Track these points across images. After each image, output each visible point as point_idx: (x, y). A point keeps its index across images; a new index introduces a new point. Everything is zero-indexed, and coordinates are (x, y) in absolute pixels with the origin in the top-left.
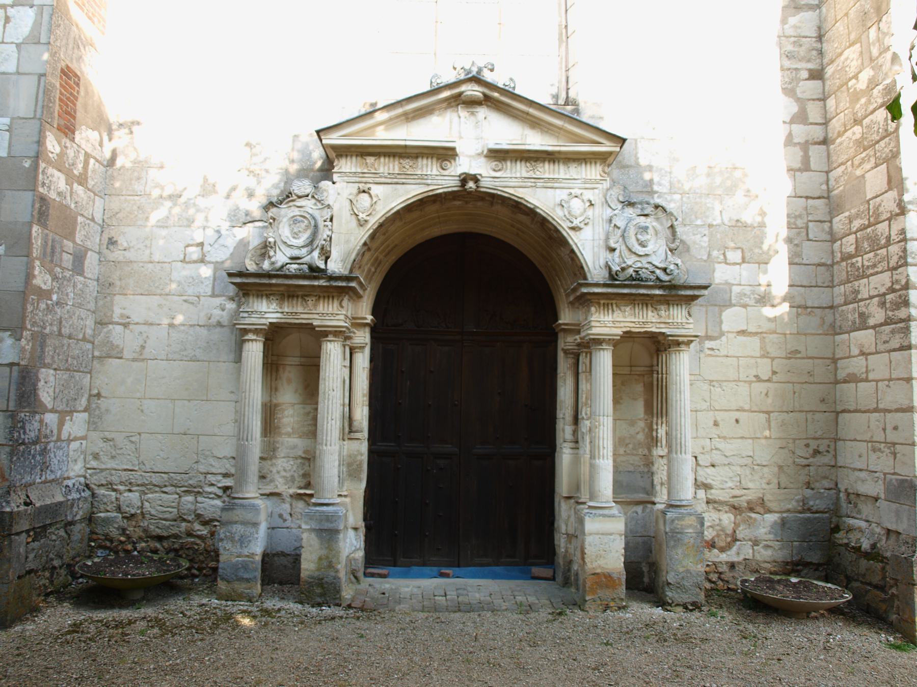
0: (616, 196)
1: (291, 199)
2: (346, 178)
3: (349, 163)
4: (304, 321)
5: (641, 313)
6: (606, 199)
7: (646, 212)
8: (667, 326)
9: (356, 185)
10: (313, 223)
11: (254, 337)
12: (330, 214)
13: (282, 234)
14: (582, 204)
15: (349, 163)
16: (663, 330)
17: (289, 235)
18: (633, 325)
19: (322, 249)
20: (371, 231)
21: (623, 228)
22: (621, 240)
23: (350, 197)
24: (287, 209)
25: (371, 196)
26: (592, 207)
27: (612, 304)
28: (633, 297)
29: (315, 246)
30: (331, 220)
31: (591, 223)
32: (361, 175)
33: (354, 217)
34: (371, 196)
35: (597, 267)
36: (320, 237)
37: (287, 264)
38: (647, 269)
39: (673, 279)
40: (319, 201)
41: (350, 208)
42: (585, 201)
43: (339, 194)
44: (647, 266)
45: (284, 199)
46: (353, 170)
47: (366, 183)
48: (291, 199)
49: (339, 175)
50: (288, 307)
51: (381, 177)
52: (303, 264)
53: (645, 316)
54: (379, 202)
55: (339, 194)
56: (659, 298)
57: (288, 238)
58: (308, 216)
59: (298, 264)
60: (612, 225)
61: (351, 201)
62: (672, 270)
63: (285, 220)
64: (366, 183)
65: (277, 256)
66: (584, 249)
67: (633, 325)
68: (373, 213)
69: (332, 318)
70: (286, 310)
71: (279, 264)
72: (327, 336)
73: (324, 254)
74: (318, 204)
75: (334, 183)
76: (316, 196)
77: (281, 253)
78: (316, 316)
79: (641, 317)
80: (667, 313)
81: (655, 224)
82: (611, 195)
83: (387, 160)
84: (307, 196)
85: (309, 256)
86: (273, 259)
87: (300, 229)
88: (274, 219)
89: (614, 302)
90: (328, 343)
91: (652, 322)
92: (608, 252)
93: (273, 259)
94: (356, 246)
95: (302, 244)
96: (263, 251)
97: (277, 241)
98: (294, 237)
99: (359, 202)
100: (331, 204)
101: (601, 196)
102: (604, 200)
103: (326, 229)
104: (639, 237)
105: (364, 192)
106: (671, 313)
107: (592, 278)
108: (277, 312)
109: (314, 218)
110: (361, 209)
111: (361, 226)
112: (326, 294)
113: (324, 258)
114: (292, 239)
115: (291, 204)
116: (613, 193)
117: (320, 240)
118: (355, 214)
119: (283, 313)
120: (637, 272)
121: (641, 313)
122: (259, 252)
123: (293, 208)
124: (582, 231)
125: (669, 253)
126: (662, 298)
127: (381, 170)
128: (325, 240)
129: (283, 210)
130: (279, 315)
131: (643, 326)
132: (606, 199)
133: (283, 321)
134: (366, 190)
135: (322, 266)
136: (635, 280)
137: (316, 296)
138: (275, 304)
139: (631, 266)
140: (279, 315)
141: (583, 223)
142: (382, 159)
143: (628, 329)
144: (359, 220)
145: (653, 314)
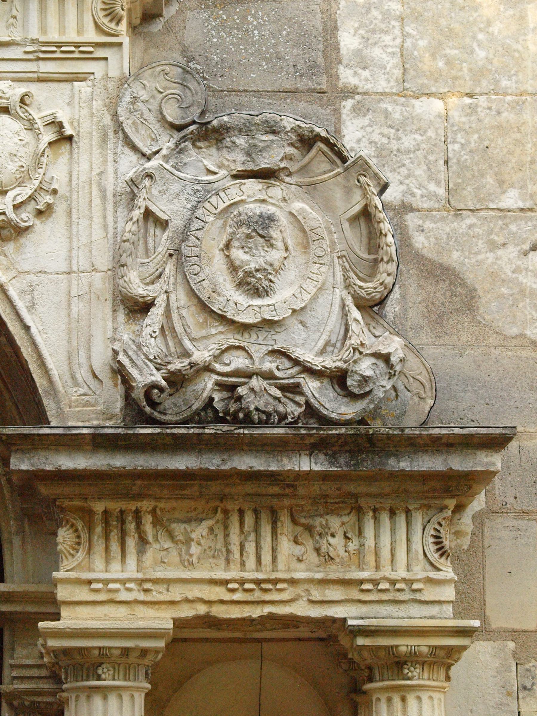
0: (154, 106)
5: (250, 547)
6: (115, 116)
7: (264, 163)
8: (355, 594)
14: (27, 136)
16: (337, 612)
18: (219, 593)
21: (177, 222)
22: (170, 268)
26: (65, 148)
27: (137, 515)
28: (215, 487)
31: (60, 209)
35: (83, 374)
38: (268, 376)
39: (375, 413)
42: (40, 124)
44: (268, 365)
53: (267, 558)
56: (316, 488)
60: (137, 214)
62: (365, 380)
66: (31, 307)
67: (219, 593)
79: (251, 562)
80: (352, 546)
81: (297, 206)
82: (135, 100)
89: (146, 505)
91: (292, 582)
92: (121, 317)
101: (98, 104)
102: (107, 120)
104: (239, 255)
106: (370, 543)
107: (60, 414)
116: (143, 95)
120: (232, 388)
121: (250, 547)
124: (26, 240)
125: (356, 313)
126: (330, 488)
131: (258, 595)
132: (115, 116)
136: (223, 421)
139: (208, 369)
141: (31, 207)
143: (202, 609)
145: (298, 550)
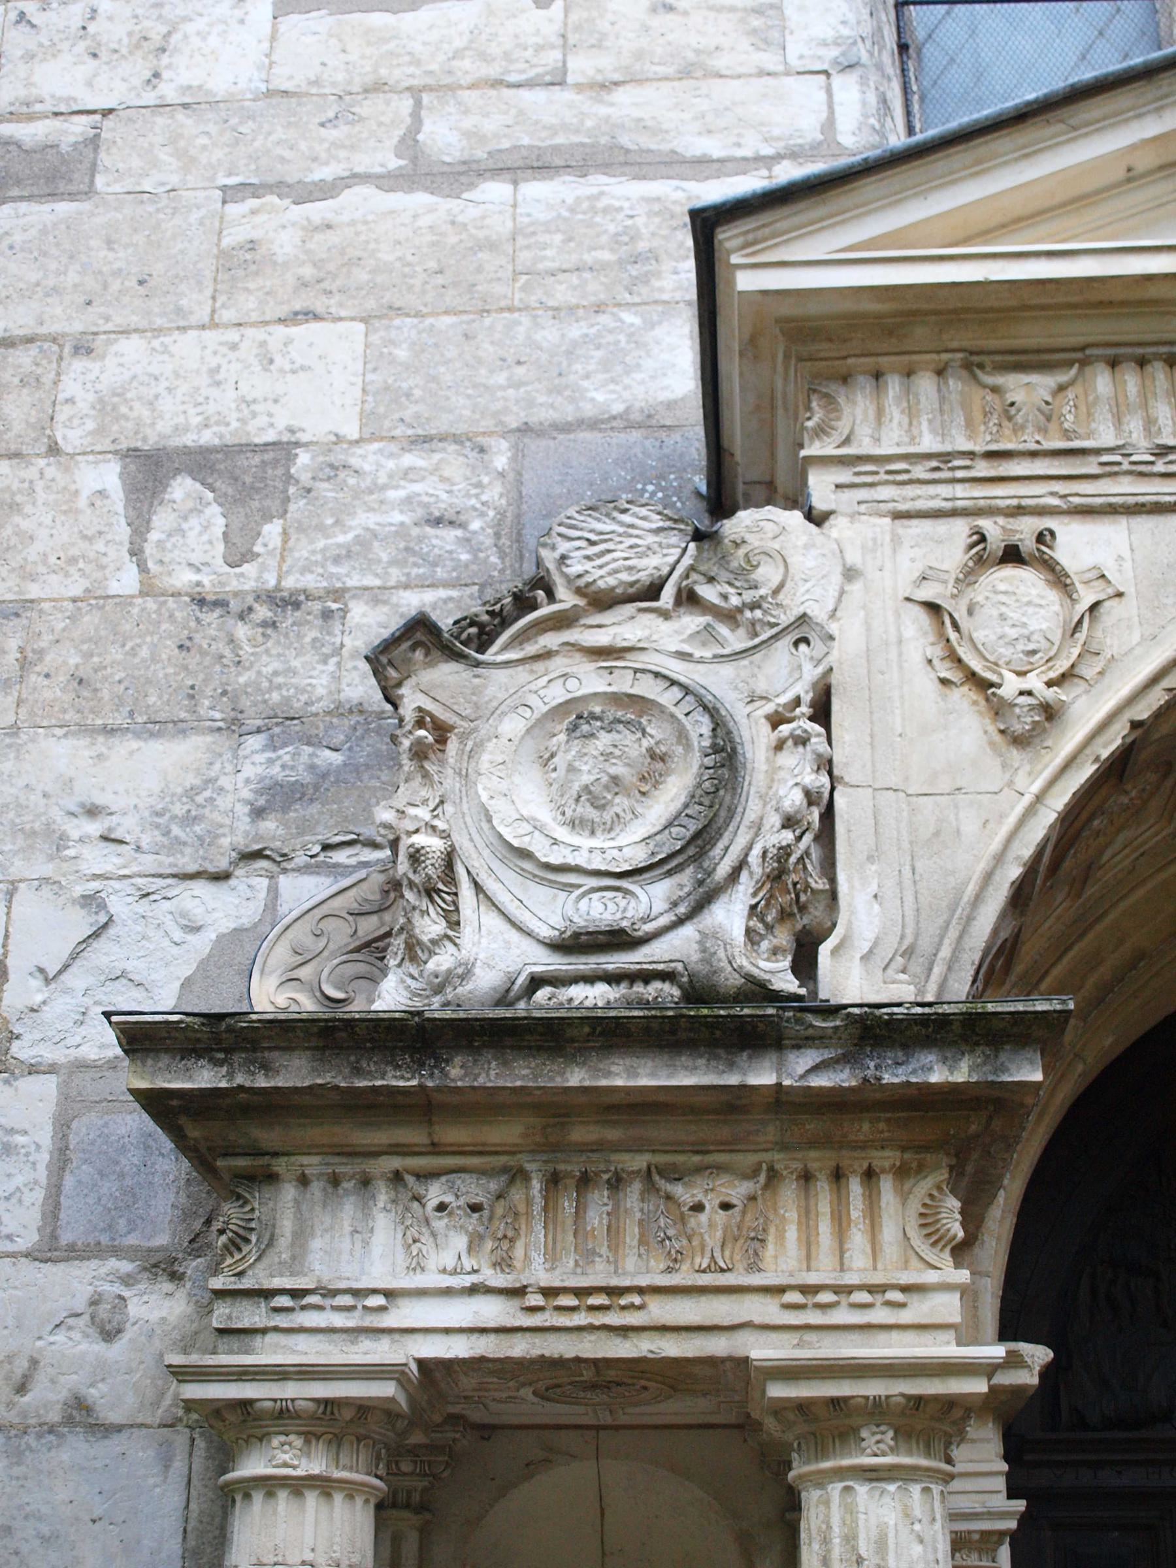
1: (545, 611)
2: (885, 492)
3: (895, 414)
4: (672, 1348)
9: (960, 529)
10: (700, 728)
11: (315, 1465)
12: (811, 673)
13: (494, 806)
15: (895, 414)
17: (546, 815)
19: (777, 876)
20: (1085, 772)
23: (927, 593)
24: (521, 674)
25: (1059, 579)
29: (723, 869)
30: (822, 712)
32: (983, 469)
33: (963, 697)
34: (1059, 579)
36: (752, 809)
37: (536, 982)
40: (730, 617)
41: (937, 652)
43: (850, 574)
45: (502, 620)
46: (929, 443)
47: (1019, 511)
48: (545, 611)
49: (845, 476)
50: (552, 1258)
51: (1111, 473)
52: (646, 977)
54: (1113, 611)
55: (850, 574)
57: (538, 827)
58: (668, 698)
59: (612, 979)
61: (933, 608)
63: (513, 726)
64: (1019, 511)
65: (467, 933)
68: (1089, 670)
69: (880, 1315)
70: (540, 1274)
71: (485, 981)
72: (847, 1436)
73: (785, 915)
74: (723, 630)
75: (816, 518)
76: (708, 592)
77: (491, 920)
78: (766, 1310)
83: (1131, 381)
84: (653, 591)
85: (688, 931)
86: (442, 961)
87: (619, 769)
88: (442, 731)
90: (862, 1490)
93: (442, 961)
94: (999, 859)
95: (639, 856)
96: (369, 927)
97: (461, 840)
98: (575, 824)
99: (989, 612)
100: (818, 613)
103: (790, 758)
105: (1012, 555)
108: (473, 1290)
109: (712, 711)
110: (1006, 652)
111: (1019, 741)
112: (818, 1160)
113: (783, 937)
114: (562, 833)
115: (551, 640)
117: (758, 827)
118: (972, 678)
119: (518, 1292)
122: (341, 934)
123: (558, 665)
127: (1106, 436)
128: (789, 822)
129: (501, 675)
130: (492, 1311)
133: (519, 1348)
134: (1028, 545)
135: (788, 983)
137: (754, 1174)
138: (460, 1242)
140: (492, 1311)
142: (1102, 381)
144: (998, 709)
